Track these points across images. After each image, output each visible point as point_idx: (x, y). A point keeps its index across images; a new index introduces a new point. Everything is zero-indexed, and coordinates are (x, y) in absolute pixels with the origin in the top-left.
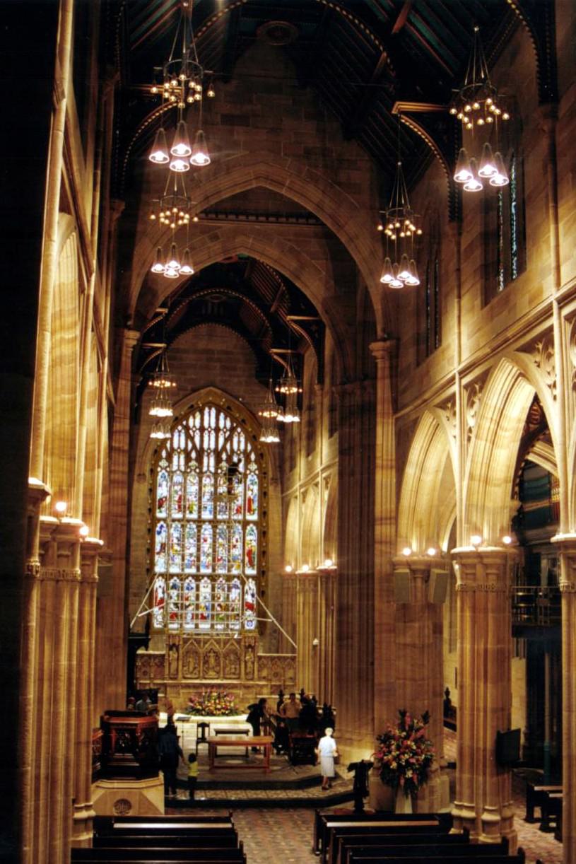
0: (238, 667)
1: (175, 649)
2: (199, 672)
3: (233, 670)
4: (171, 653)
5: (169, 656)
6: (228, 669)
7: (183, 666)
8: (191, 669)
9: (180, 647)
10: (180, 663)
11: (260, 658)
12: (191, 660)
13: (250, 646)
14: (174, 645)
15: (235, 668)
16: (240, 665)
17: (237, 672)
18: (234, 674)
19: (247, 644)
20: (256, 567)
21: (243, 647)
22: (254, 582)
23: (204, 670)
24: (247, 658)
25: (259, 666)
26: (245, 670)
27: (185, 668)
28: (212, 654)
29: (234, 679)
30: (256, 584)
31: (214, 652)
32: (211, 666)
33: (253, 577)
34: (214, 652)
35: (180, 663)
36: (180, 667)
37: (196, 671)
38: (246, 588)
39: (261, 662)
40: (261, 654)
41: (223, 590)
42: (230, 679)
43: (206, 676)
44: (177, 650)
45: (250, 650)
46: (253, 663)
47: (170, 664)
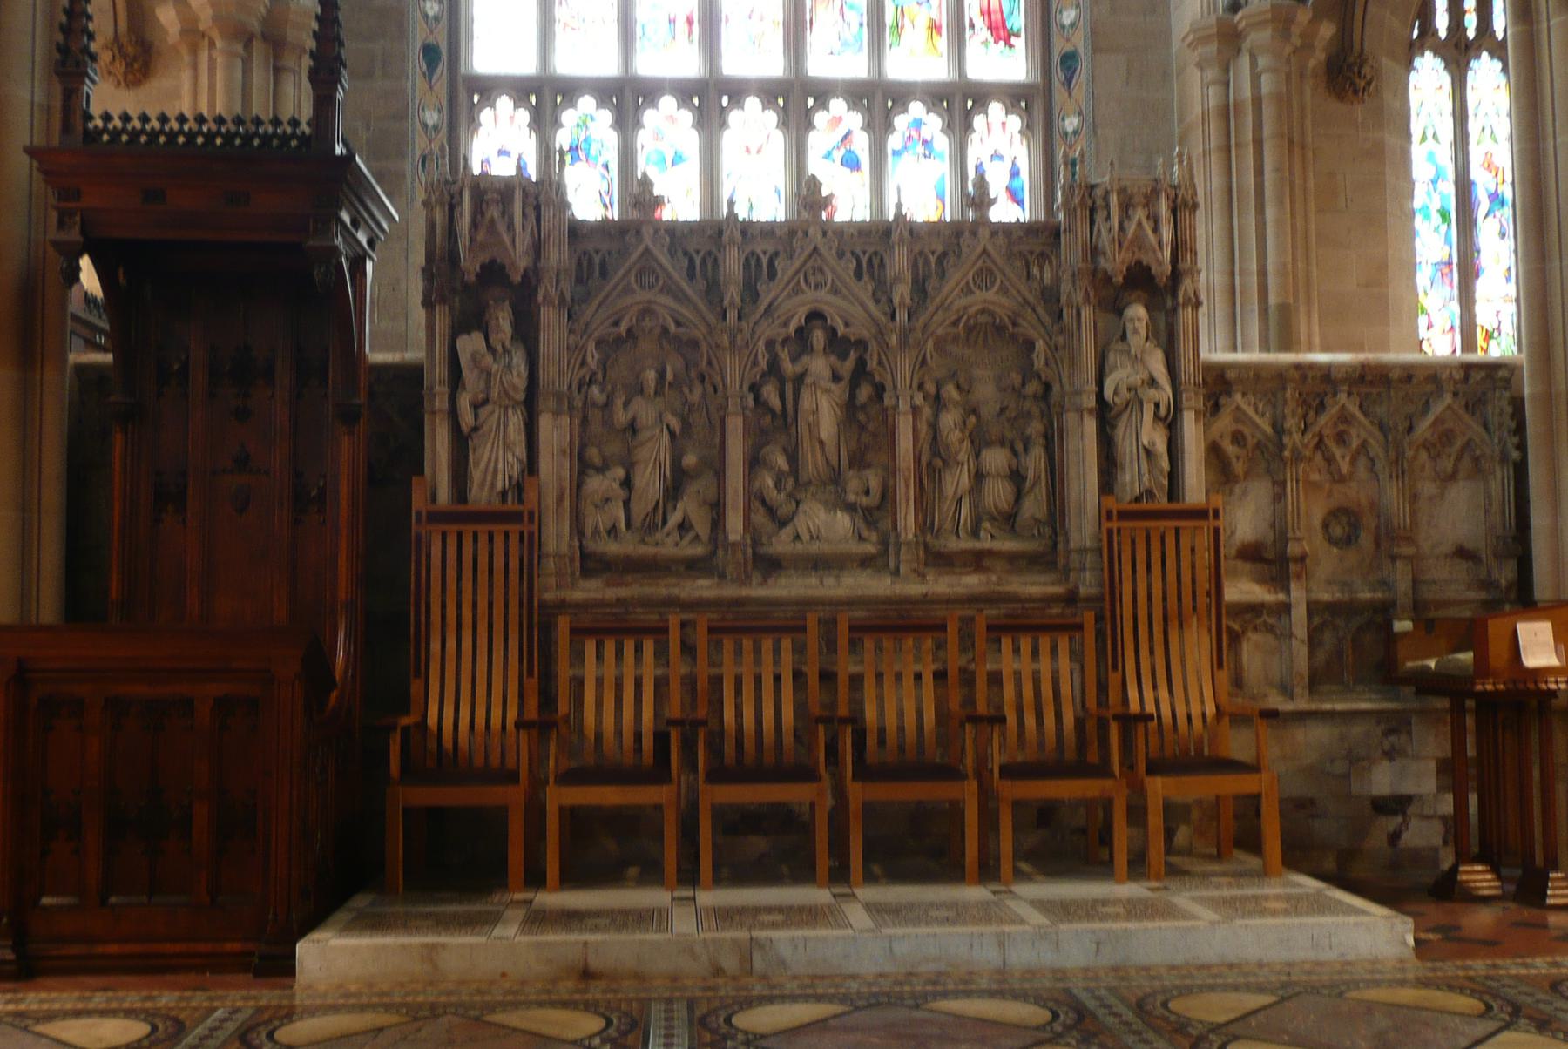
0: (1035, 462)
1: (503, 321)
2: (717, 509)
3: (998, 493)
4: (469, 344)
5: (455, 379)
6: (957, 481)
7: (583, 467)
8: (649, 483)
9: (548, 289)
10: (554, 432)
11: (1219, 382)
12: (644, 410)
13: (1140, 280)
14: (493, 273)
15: (1016, 476)
16: (1053, 441)
17: (1034, 506)
18: (1009, 520)
19: (1115, 263)
20: (1019, 43)
21: (1073, 292)
22: (1015, 122)
23: (753, 498)
24: (1120, 377)
25: (1214, 451)
26: (1107, 483)
27: (596, 484)
28: (819, 366)
29: (1015, 561)
30: (1027, 130)
31: (837, 344)
32: (813, 463)
33: (1014, 96)
34: (837, 344)
35: (554, 432)
36: (553, 468)
37: (689, 506)
38: (977, 150)
39: (1224, 423)
40: (1215, 352)
41: (851, 163)
42: (978, 561)
43: (781, 544)
44: (526, 332)
45: (1138, 312)
46: (1171, 425)
47: (461, 442)
